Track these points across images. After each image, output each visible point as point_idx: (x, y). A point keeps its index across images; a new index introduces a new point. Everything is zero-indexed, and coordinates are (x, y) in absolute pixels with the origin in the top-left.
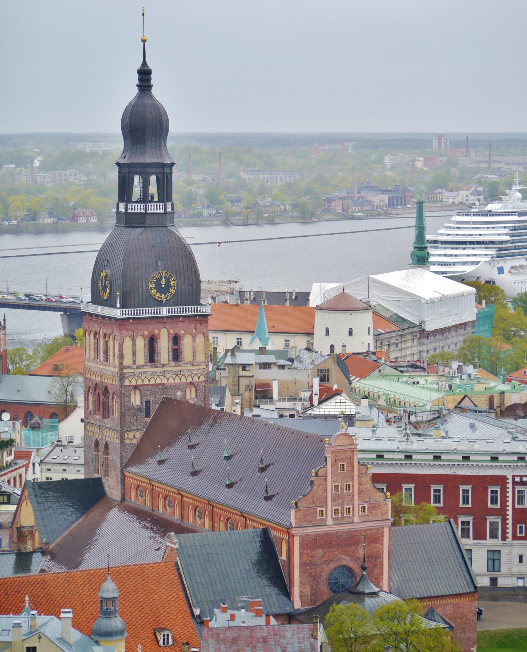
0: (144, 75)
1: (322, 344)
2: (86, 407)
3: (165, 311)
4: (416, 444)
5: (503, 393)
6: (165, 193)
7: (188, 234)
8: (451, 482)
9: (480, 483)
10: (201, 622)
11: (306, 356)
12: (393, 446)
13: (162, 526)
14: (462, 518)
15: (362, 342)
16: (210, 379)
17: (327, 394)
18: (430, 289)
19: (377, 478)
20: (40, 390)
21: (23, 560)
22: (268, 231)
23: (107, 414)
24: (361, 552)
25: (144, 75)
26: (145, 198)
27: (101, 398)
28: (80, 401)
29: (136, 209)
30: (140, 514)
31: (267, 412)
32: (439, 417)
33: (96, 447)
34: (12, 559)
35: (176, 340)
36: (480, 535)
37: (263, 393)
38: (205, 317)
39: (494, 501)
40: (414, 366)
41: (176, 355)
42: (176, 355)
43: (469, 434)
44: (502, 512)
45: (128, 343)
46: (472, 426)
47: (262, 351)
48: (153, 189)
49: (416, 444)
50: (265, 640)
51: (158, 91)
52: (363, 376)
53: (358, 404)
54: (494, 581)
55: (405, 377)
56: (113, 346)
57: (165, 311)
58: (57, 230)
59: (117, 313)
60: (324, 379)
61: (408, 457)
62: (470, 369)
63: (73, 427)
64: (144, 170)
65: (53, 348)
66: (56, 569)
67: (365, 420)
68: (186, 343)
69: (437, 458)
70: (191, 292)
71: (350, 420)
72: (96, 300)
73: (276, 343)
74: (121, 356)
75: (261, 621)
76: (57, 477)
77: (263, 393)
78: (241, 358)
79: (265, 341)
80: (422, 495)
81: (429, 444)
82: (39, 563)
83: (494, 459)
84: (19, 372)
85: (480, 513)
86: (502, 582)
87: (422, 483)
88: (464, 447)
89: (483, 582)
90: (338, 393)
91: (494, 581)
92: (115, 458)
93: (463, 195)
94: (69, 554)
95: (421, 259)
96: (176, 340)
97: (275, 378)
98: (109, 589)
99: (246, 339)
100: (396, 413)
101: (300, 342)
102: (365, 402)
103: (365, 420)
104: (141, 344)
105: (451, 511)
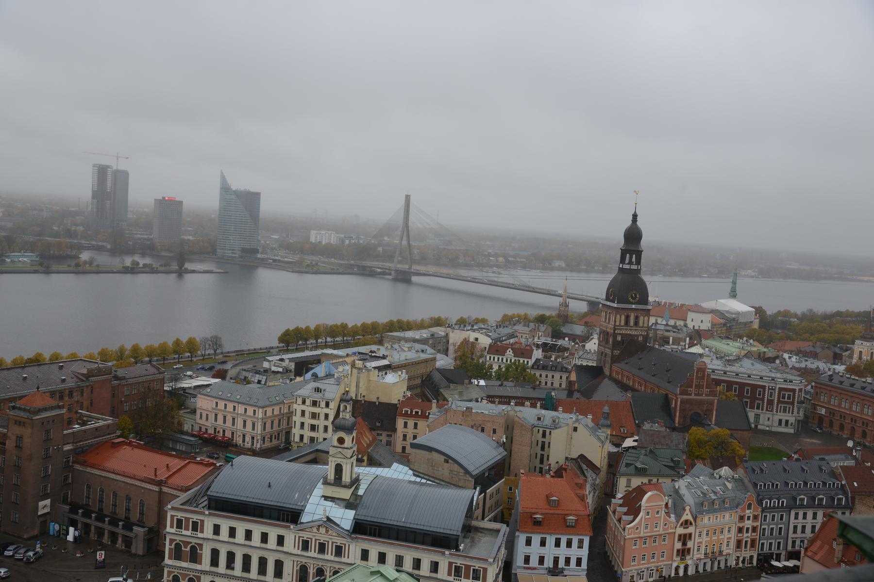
0: (635, 216)
1: (690, 325)
2: (599, 339)
3: (634, 306)
4: (728, 368)
5: (765, 352)
6: (638, 262)
7: (646, 278)
8: (742, 385)
9: (754, 387)
10: (638, 426)
11: (685, 329)
12: (719, 368)
13: (625, 387)
14: (745, 400)
15: (706, 326)
16: (648, 334)
17: (691, 345)
18: (737, 306)
19: (714, 380)
20: (579, 330)
21: (570, 393)
22: (667, 279)
23: (607, 342)
24: (705, 408)
25: (635, 216)
26: (630, 263)
27: (605, 337)
28: (596, 336)
29: (627, 267)
30: (616, 382)
31: (668, 348)
32: (738, 359)
33: (601, 354)
34: (566, 392)
35: (637, 318)
36: (752, 407)
37: (666, 341)
38: (649, 310)
39: (759, 395)
40: (728, 338)
41: (636, 323)
42: (636, 323)
43: (750, 366)
44: (763, 400)
45: (618, 316)
46: (752, 364)
47: (667, 325)
48: (634, 260)
49: (728, 368)
50: (664, 437)
51: (639, 223)
52: (706, 339)
53: (704, 349)
54: (756, 426)
55: (724, 341)
56: (612, 318)
57: (634, 306)
58: (587, 271)
59: (615, 305)
60: (690, 339)
61: (725, 373)
62: (751, 341)
63: (593, 345)
64: (631, 252)
65: (585, 315)
66: (583, 399)
67: (707, 356)
68: (641, 318)
69: (737, 375)
70: (644, 300)
71: (701, 355)
72: (607, 299)
73: (672, 322)
74: (615, 321)
75: (663, 429)
76: (585, 364)
77: (666, 341)
78: (658, 327)
79: (667, 321)
80: (729, 389)
81: (736, 368)
82: (576, 395)
83: (761, 378)
84: (571, 323)
85: (753, 398)
86: (759, 427)
87: (730, 385)
88: (749, 372)
89: (753, 426)
90: (696, 345)
91: (756, 426)
92: (609, 359)
93: (749, 272)
94: (587, 393)
95: (733, 295)
96: (637, 318)
97: (671, 336)
98: (606, 409)
99: (660, 320)
100: (720, 356)
101: (680, 323)
102: (707, 349)
103: (707, 356)
104: (623, 317)
105: (741, 395)
